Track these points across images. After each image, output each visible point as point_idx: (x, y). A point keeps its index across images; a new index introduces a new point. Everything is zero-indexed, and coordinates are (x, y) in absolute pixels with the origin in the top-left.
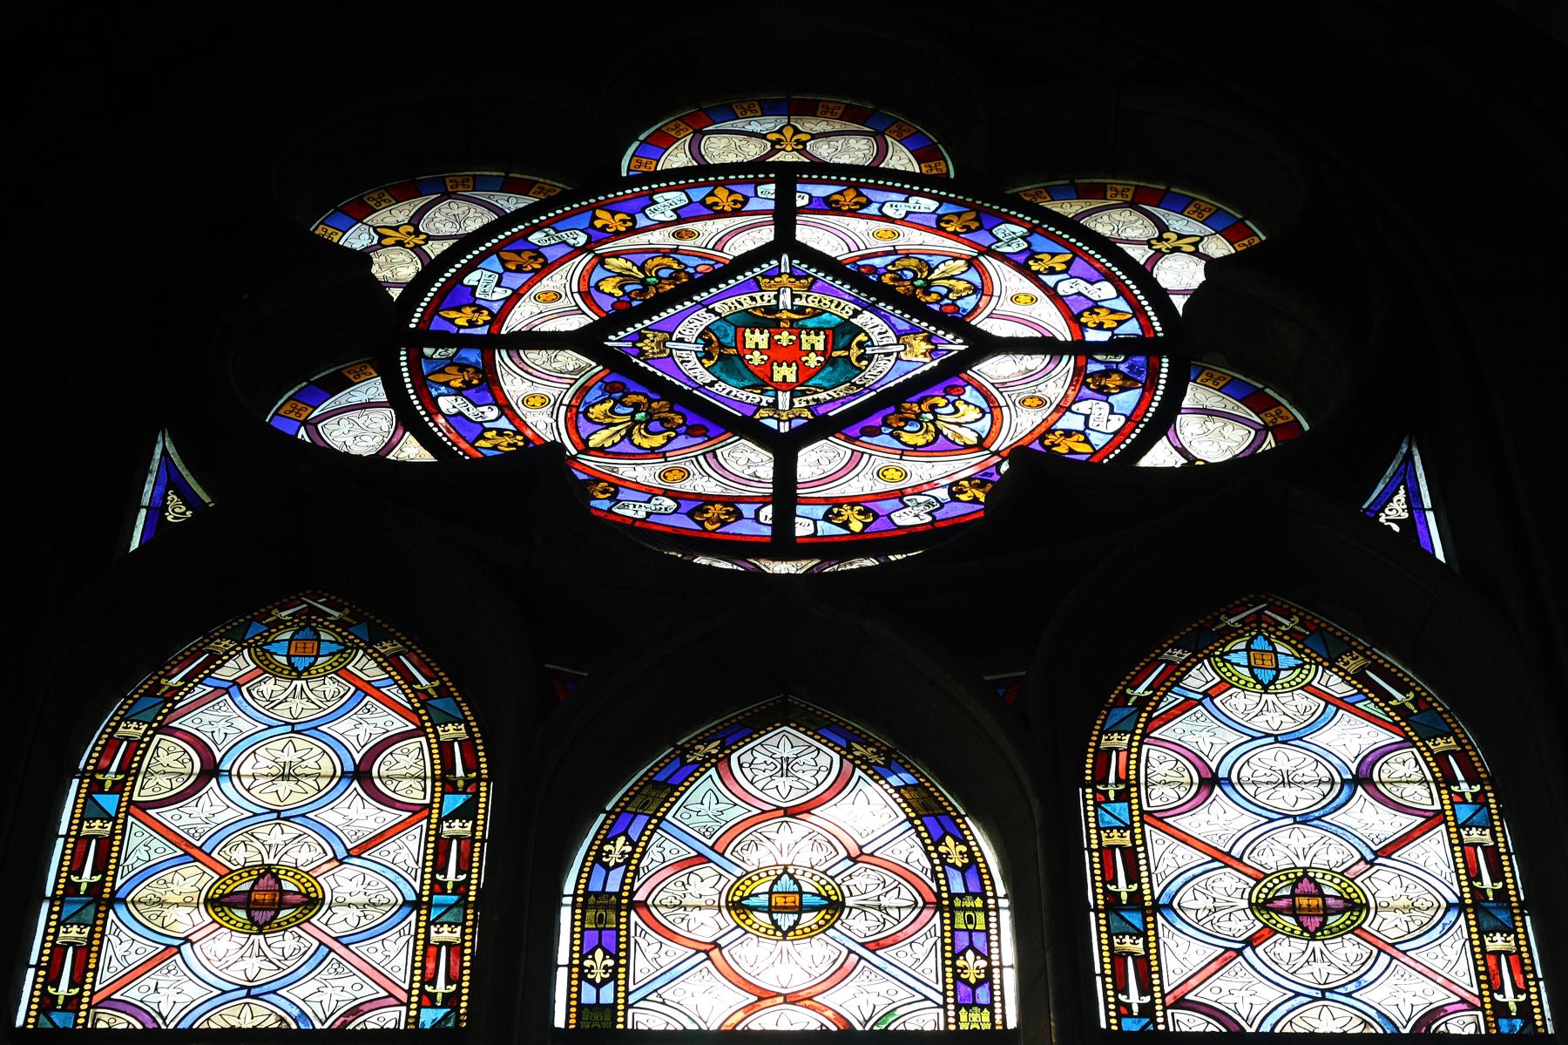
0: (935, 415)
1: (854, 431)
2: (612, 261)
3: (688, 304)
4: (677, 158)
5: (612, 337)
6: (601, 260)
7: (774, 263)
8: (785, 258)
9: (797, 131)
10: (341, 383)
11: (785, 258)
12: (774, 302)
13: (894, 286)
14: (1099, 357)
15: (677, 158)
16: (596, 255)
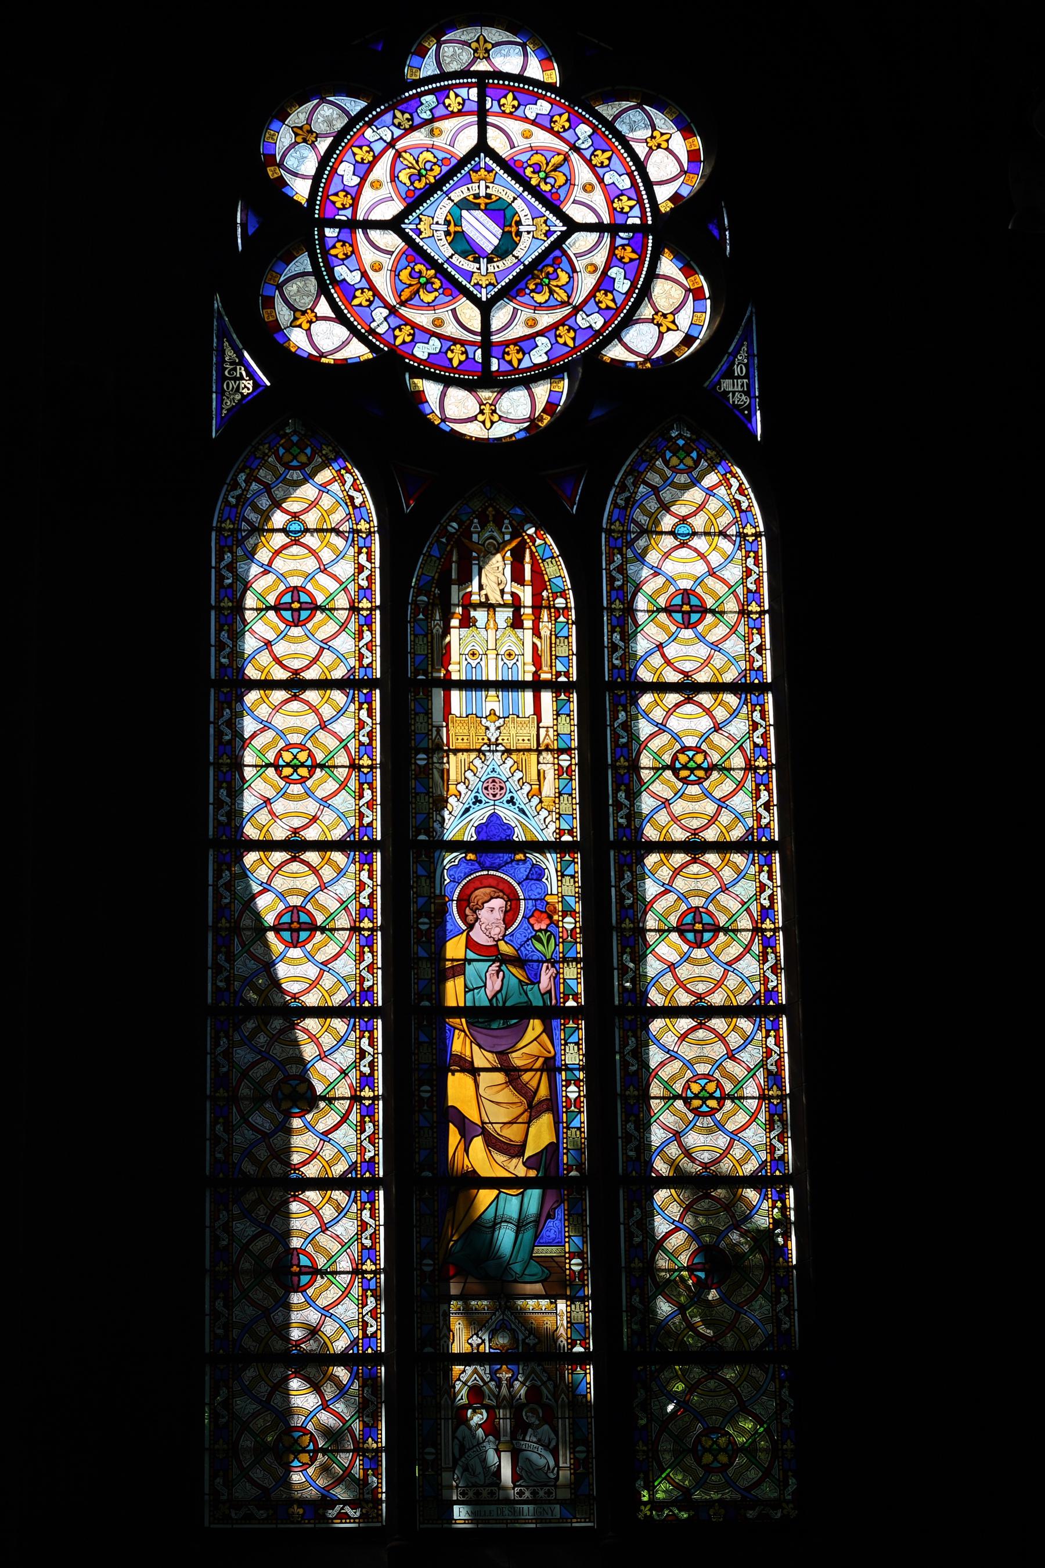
0: (550, 280)
1: (513, 293)
2: (404, 154)
3: (439, 193)
4: (428, 68)
5: (406, 221)
6: (398, 155)
7: (477, 159)
8: (482, 155)
9: (486, 41)
10: (289, 259)
11: (482, 155)
12: (477, 191)
13: (531, 178)
14: (621, 234)
15: (428, 68)
16: (397, 150)
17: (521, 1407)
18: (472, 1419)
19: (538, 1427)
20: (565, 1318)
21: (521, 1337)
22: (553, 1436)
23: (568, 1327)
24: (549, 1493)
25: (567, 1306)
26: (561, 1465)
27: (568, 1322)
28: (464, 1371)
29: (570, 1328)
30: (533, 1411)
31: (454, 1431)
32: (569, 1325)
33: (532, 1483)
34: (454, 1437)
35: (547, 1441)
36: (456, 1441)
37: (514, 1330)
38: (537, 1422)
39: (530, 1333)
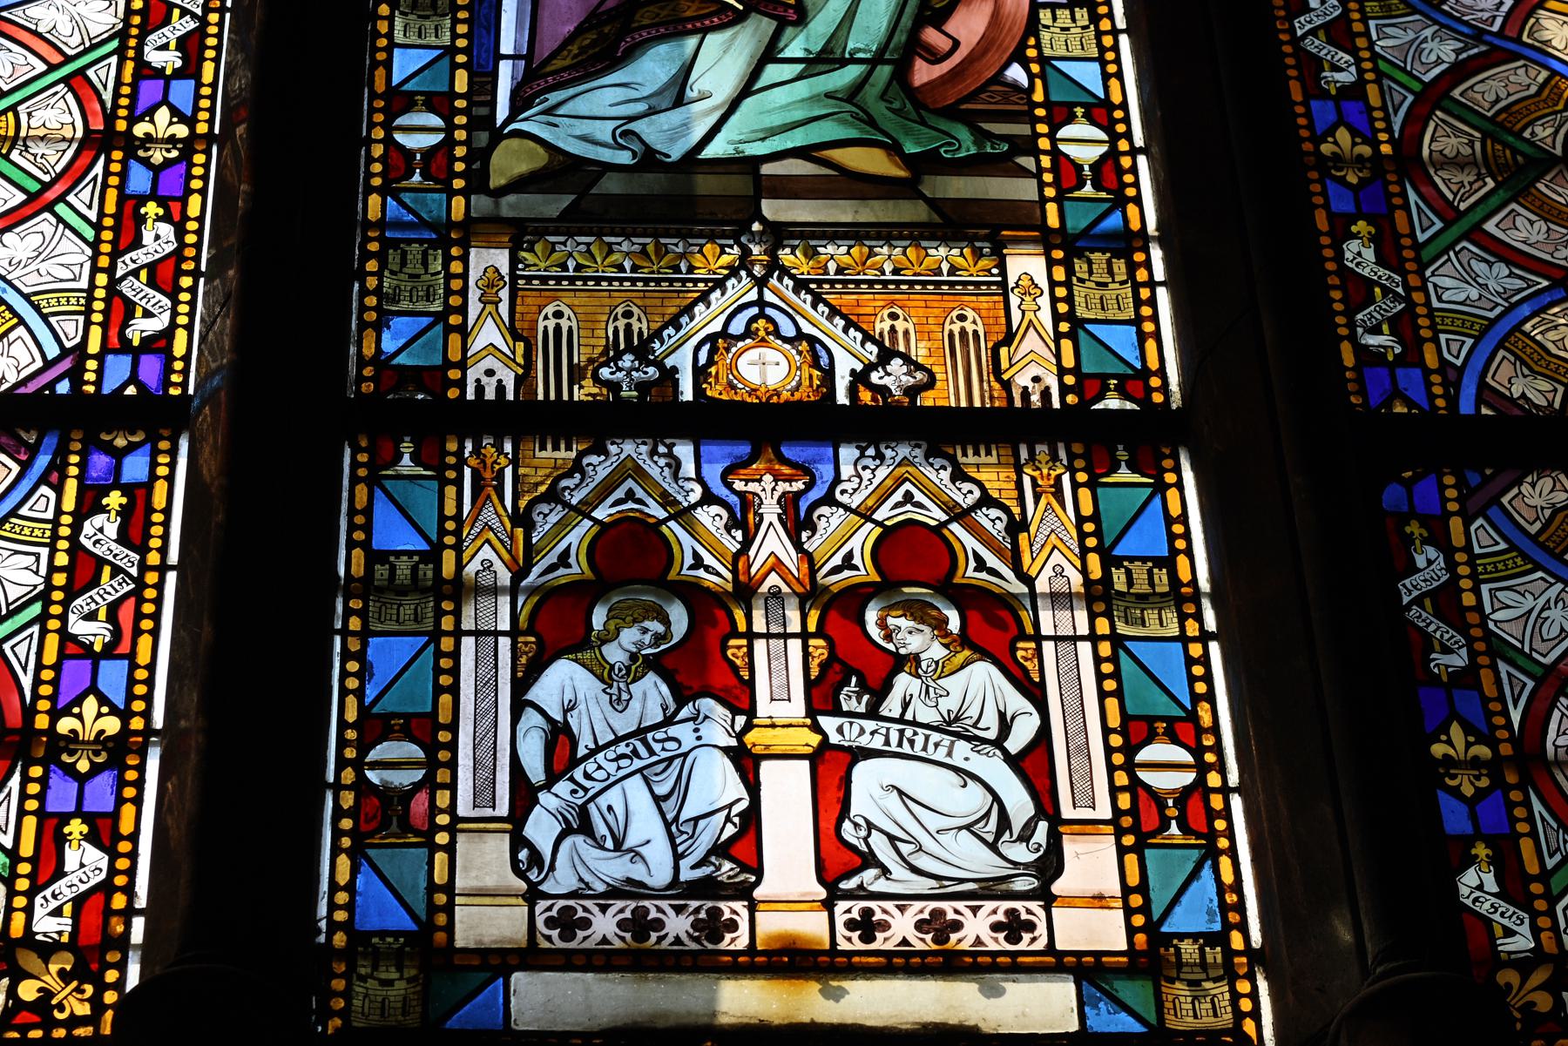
17: (856, 597)
18: (609, 636)
19: (943, 670)
20: (1045, 301)
21: (845, 367)
22: (1016, 702)
23: (1058, 336)
24: (1014, 927)
25: (1051, 263)
26: (1067, 812)
27: (1057, 318)
28: (577, 467)
29: (1072, 335)
30: (919, 612)
31: (521, 686)
32: (1064, 327)
33: (924, 885)
34: (519, 705)
35: (991, 723)
36: (531, 718)
37: (812, 340)
38: (937, 651)
39: (886, 356)
